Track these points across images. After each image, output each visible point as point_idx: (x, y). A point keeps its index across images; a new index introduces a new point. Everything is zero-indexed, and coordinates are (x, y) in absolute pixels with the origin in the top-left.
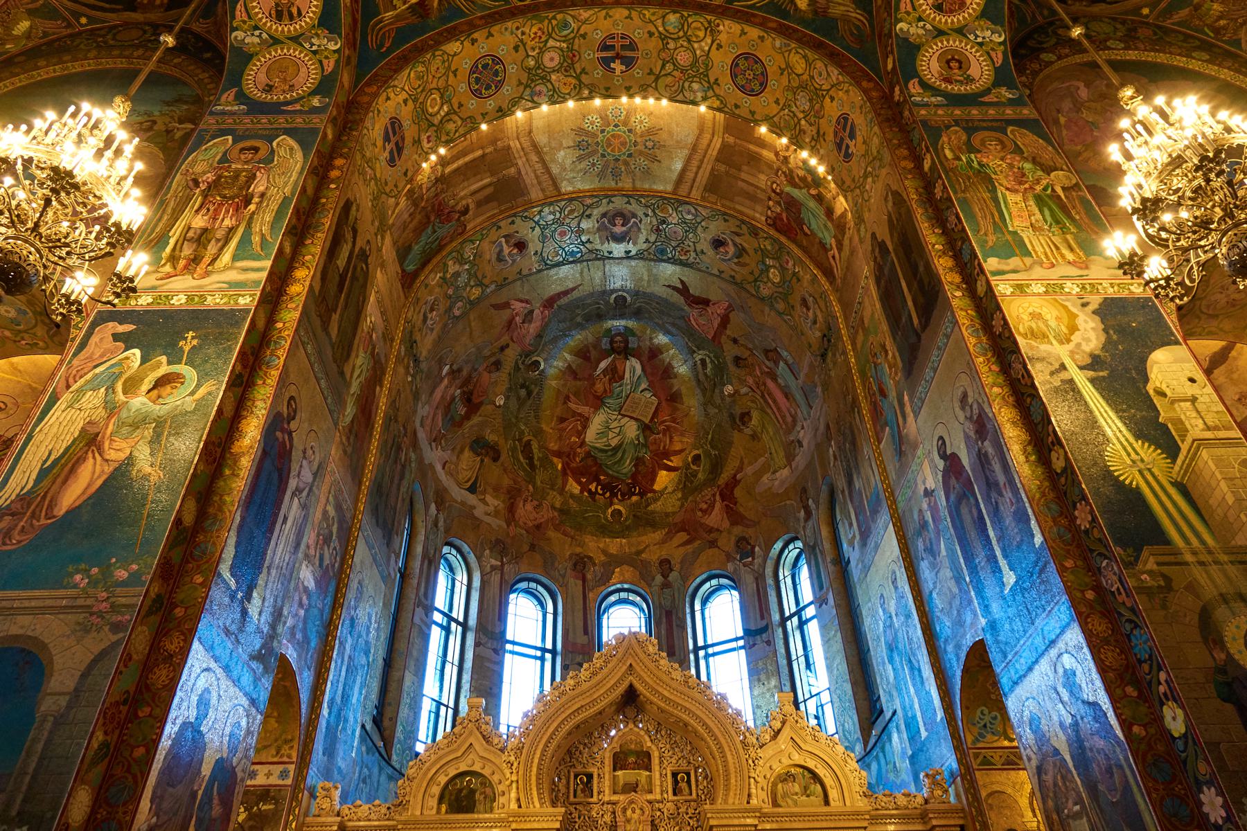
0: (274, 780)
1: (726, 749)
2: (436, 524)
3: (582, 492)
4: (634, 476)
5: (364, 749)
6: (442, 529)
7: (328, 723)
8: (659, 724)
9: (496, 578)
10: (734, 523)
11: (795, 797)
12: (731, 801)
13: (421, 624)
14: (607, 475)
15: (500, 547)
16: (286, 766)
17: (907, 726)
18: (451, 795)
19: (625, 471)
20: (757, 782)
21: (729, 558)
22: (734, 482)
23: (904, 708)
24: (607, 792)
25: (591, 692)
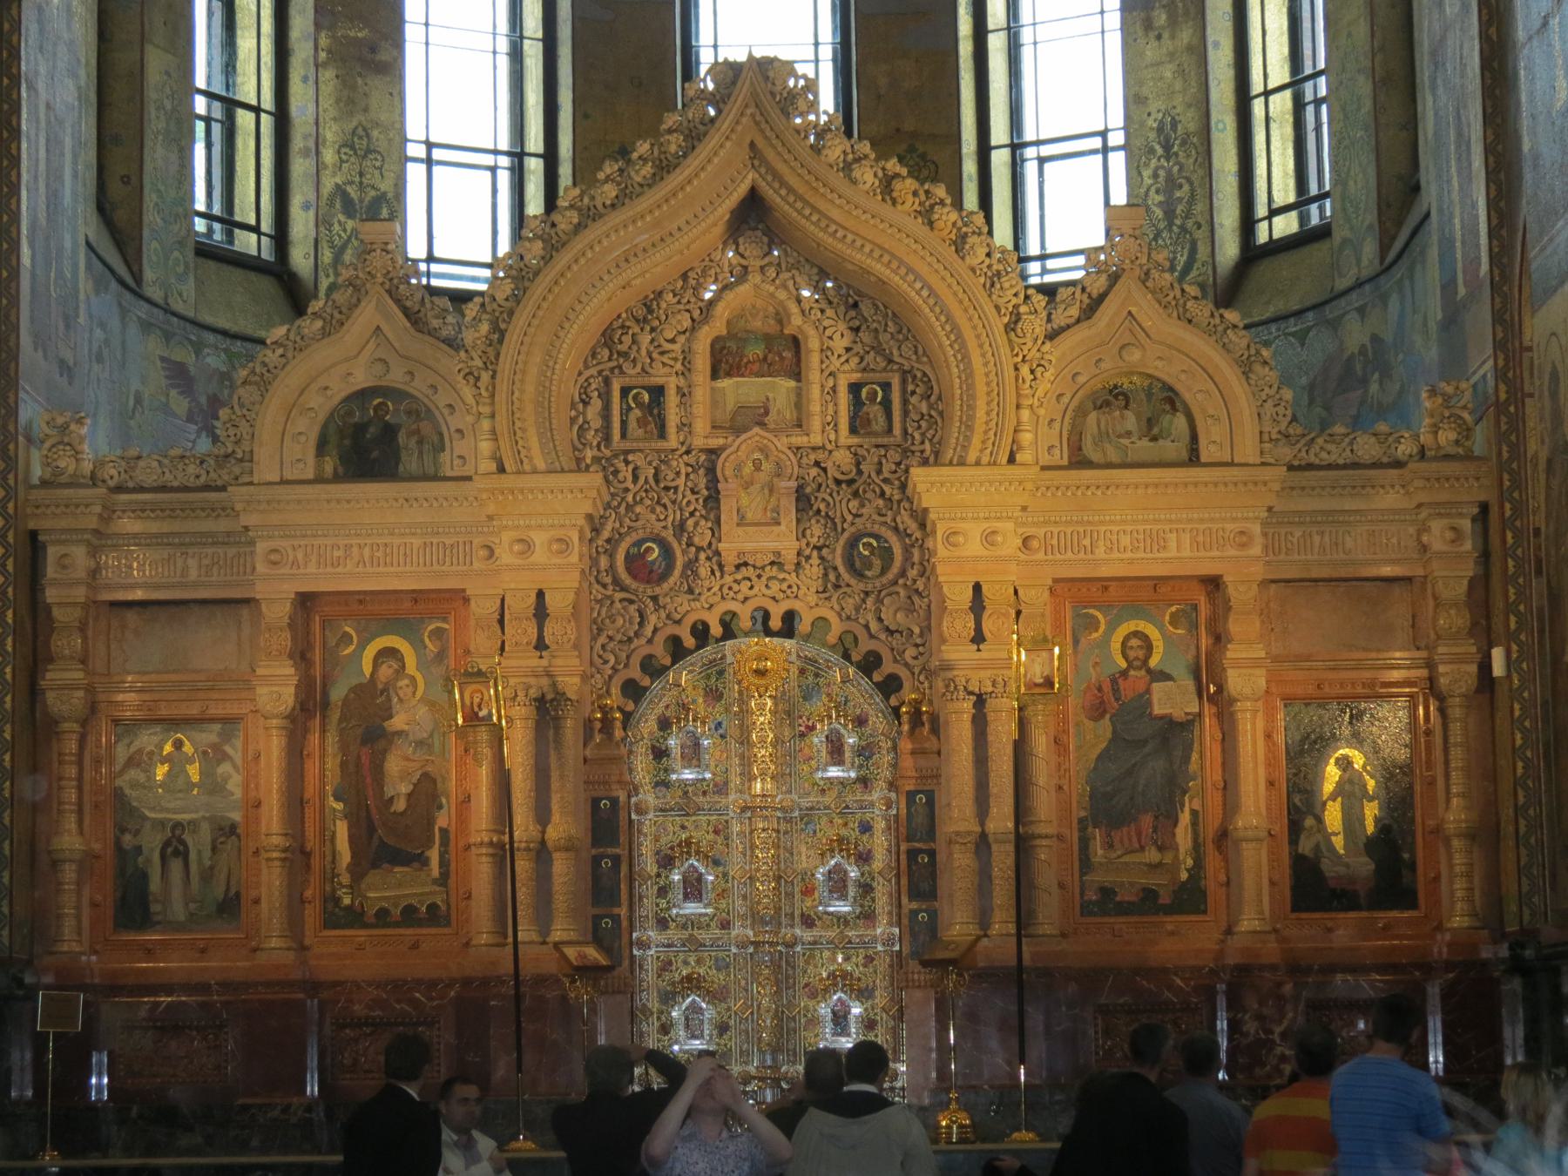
1: (972, 344)
5: (90, 285)
7: (33, 275)
11: (1125, 441)
23: (1440, 210)
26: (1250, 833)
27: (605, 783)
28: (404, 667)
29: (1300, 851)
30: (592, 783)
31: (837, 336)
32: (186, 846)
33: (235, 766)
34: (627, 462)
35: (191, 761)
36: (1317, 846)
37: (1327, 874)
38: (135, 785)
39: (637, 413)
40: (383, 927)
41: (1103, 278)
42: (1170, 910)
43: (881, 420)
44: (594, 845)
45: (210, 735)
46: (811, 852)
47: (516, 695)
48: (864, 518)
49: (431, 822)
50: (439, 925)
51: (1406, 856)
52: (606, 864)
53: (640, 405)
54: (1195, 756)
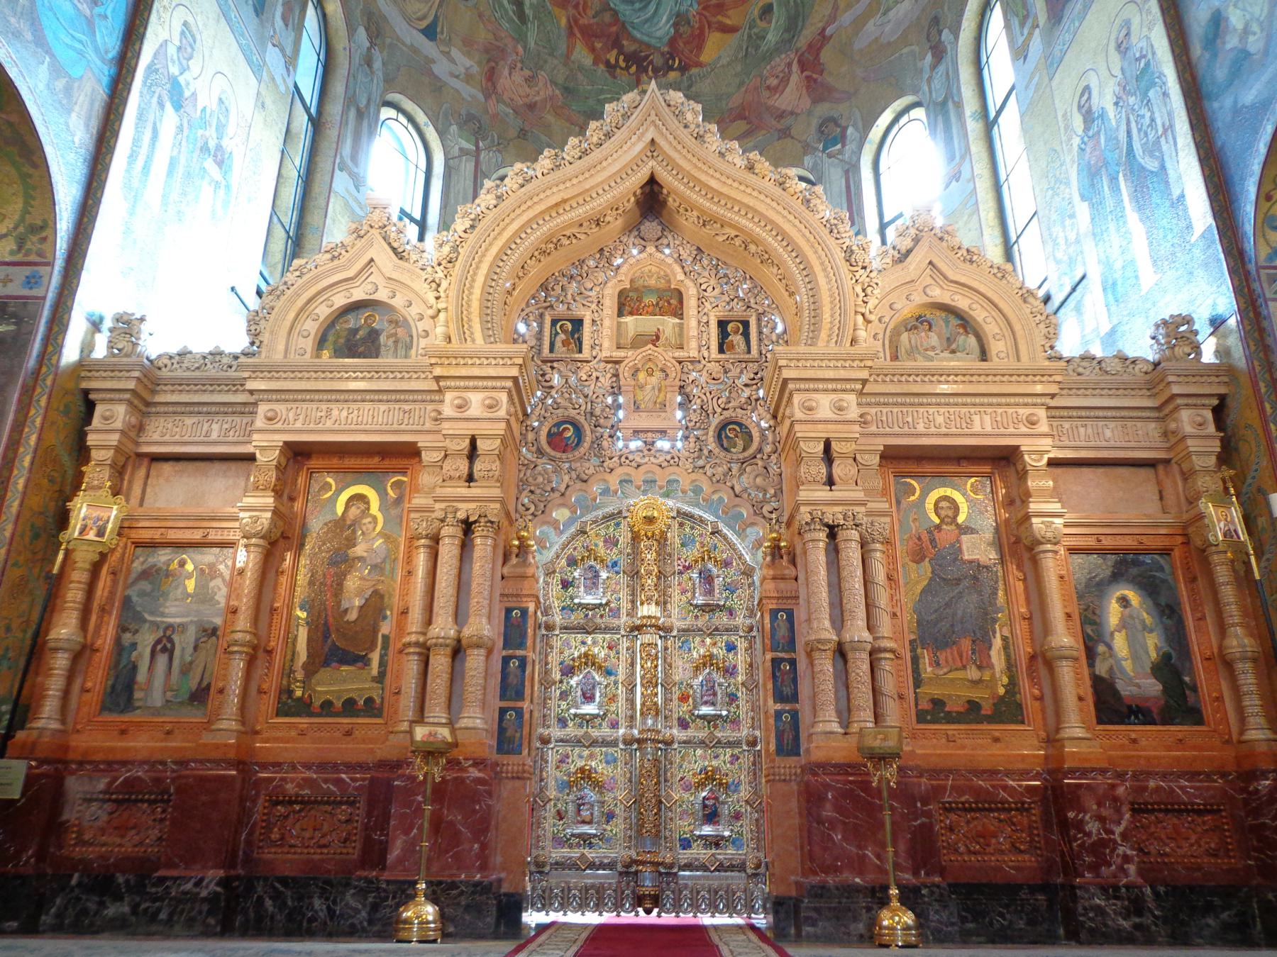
0: (15, 289)
1: (817, 269)
2: (369, 62)
3: (596, 62)
4: (672, 42)
6: (380, 74)
8: (699, 249)
9: (467, 167)
10: (815, 101)
11: (931, 353)
12: (821, 343)
13: (347, 197)
14: (635, 40)
15: (475, 126)
16: (36, 268)
17: (1109, 286)
18: (339, 337)
19: (659, 34)
20: (868, 322)
21: (807, 149)
22: (823, 38)
24: (606, 344)
25: (581, 178)
26: (1067, 653)
27: (518, 596)
28: (368, 509)
29: (1097, 673)
30: (507, 596)
31: (710, 289)
32: (173, 645)
33: (224, 580)
34: (552, 368)
35: (189, 576)
36: (1111, 668)
37: (1122, 693)
38: (142, 594)
39: (562, 336)
40: (327, 715)
41: (909, 240)
42: (991, 719)
43: (743, 346)
44: (504, 648)
45: (209, 556)
46: (687, 666)
47: (445, 517)
48: (730, 411)
49: (375, 630)
50: (376, 716)
51: (1187, 679)
52: (514, 664)
53: (564, 332)
54: (1001, 593)
